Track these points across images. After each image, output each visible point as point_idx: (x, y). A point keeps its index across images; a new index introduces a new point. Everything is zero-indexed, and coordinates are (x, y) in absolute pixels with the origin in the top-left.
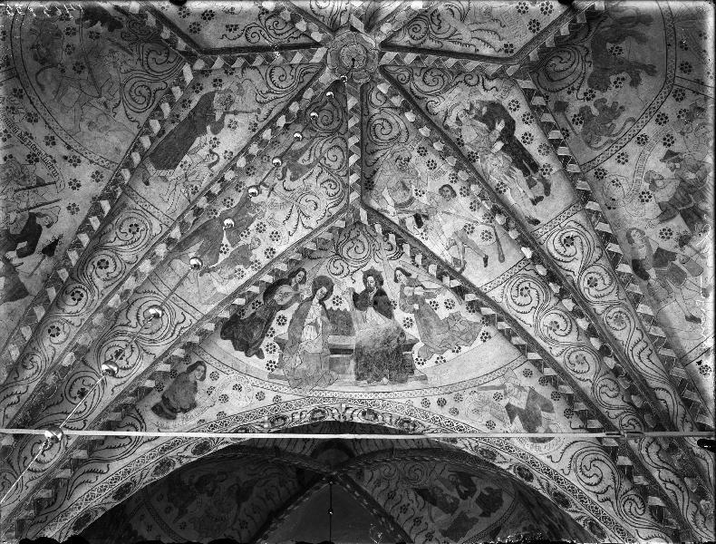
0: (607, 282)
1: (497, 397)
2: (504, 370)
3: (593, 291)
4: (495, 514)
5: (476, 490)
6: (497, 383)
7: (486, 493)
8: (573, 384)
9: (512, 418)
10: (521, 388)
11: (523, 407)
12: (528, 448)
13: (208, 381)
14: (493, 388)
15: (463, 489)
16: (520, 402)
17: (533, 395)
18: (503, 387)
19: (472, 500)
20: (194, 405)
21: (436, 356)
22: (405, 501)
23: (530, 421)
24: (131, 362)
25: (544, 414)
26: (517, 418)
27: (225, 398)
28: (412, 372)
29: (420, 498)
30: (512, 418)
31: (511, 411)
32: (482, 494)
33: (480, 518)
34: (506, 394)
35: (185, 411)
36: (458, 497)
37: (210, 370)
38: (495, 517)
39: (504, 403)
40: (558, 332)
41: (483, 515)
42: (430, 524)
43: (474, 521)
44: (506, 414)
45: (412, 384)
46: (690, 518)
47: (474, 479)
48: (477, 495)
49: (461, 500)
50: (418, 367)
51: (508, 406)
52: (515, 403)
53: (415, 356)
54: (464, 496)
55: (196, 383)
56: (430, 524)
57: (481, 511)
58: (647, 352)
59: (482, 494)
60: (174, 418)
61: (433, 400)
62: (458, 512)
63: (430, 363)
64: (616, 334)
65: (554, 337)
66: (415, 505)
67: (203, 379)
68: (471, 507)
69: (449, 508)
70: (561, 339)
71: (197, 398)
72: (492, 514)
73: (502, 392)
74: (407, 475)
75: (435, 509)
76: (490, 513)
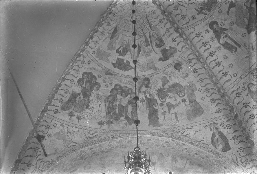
4: (118, 70)
5: (124, 56)
7: (125, 61)
15: (121, 50)
19: (118, 56)
22: (112, 23)
29: (113, 30)
32: (123, 60)
33: (111, 63)
36: (117, 49)
38: (116, 70)
41: (113, 64)
42: (102, 41)
43: (109, 61)
47: (129, 53)
48: (121, 57)
49: (115, 51)
54: (118, 51)
56: (102, 41)
57: (114, 62)
59: (123, 60)
62: (109, 51)
66: (110, 29)
68: (114, 57)
69: (110, 47)
72: (117, 68)
74: (123, 19)
75: (108, 40)
76: (116, 67)
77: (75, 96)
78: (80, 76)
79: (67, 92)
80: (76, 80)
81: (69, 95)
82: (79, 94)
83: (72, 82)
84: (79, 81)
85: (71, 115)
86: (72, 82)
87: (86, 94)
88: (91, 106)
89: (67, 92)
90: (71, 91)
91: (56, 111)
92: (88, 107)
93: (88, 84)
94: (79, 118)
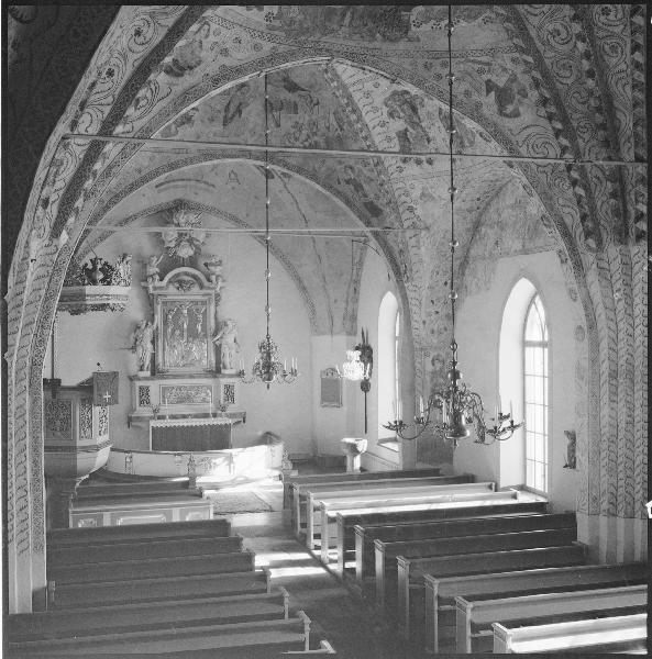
0: (619, 16)
1: (480, 72)
2: (493, 52)
3: (603, 18)
6: (485, 59)
8: (552, 88)
9: (488, 92)
10: (505, 70)
11: (501, 85)
12: (496, 118)
13: (212, 38)
14: (480, 63)
16: (501, 81)
17: (513, 79)
18: (488, 64)
20: (199, 63)
21: (433, 22)
23: (503, 97)
24: (149, 36)
25: (518, 97)
26: (493, 93)
27: (225, 52)
28: (406, 33)
30: (488, 92)
31: (490, 86)
34: (489, 71)
35: (191, 68)
37: (214, 27)
39: (486, 77)
40: (557, 39)
44: (484, 88)
45: (402, 45)
46: (599, 204)
50: (413, 29)
51: (489, 81)
52: (494, 79)
53: (413, 18)
55: (201, 42)
58: (624, 81)
60: (182, 75)
61: (421, 62)
63: (426, 27)
64: (606, 57)
65: (552, 41)
67: (207, 36)
70: (557, 46)
71: (203, 54)
73: (486, 68)
77: (403, 135)
78: (385, 110)
79: (389, 139)
80: (385, 117)
81: (396, 141)
82: (406, 130)
83: (383, 124)
84: (391, 115)
85: (419, 162)
86: (383, 124)
87: (416, 124)
88: (431, 135)
89: (389, 139)
90: (394, 135)
91: (401, 170)
92: (429, 141)
93: (405, 107)
94: (430, 162)
